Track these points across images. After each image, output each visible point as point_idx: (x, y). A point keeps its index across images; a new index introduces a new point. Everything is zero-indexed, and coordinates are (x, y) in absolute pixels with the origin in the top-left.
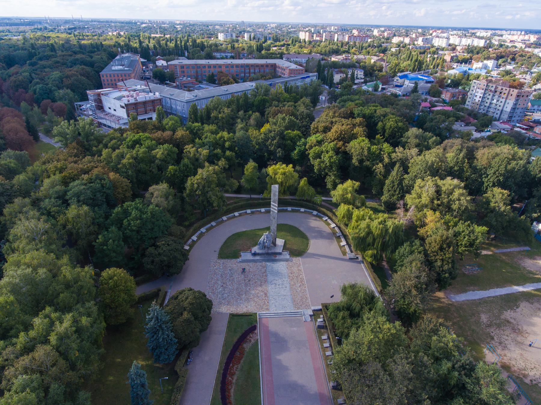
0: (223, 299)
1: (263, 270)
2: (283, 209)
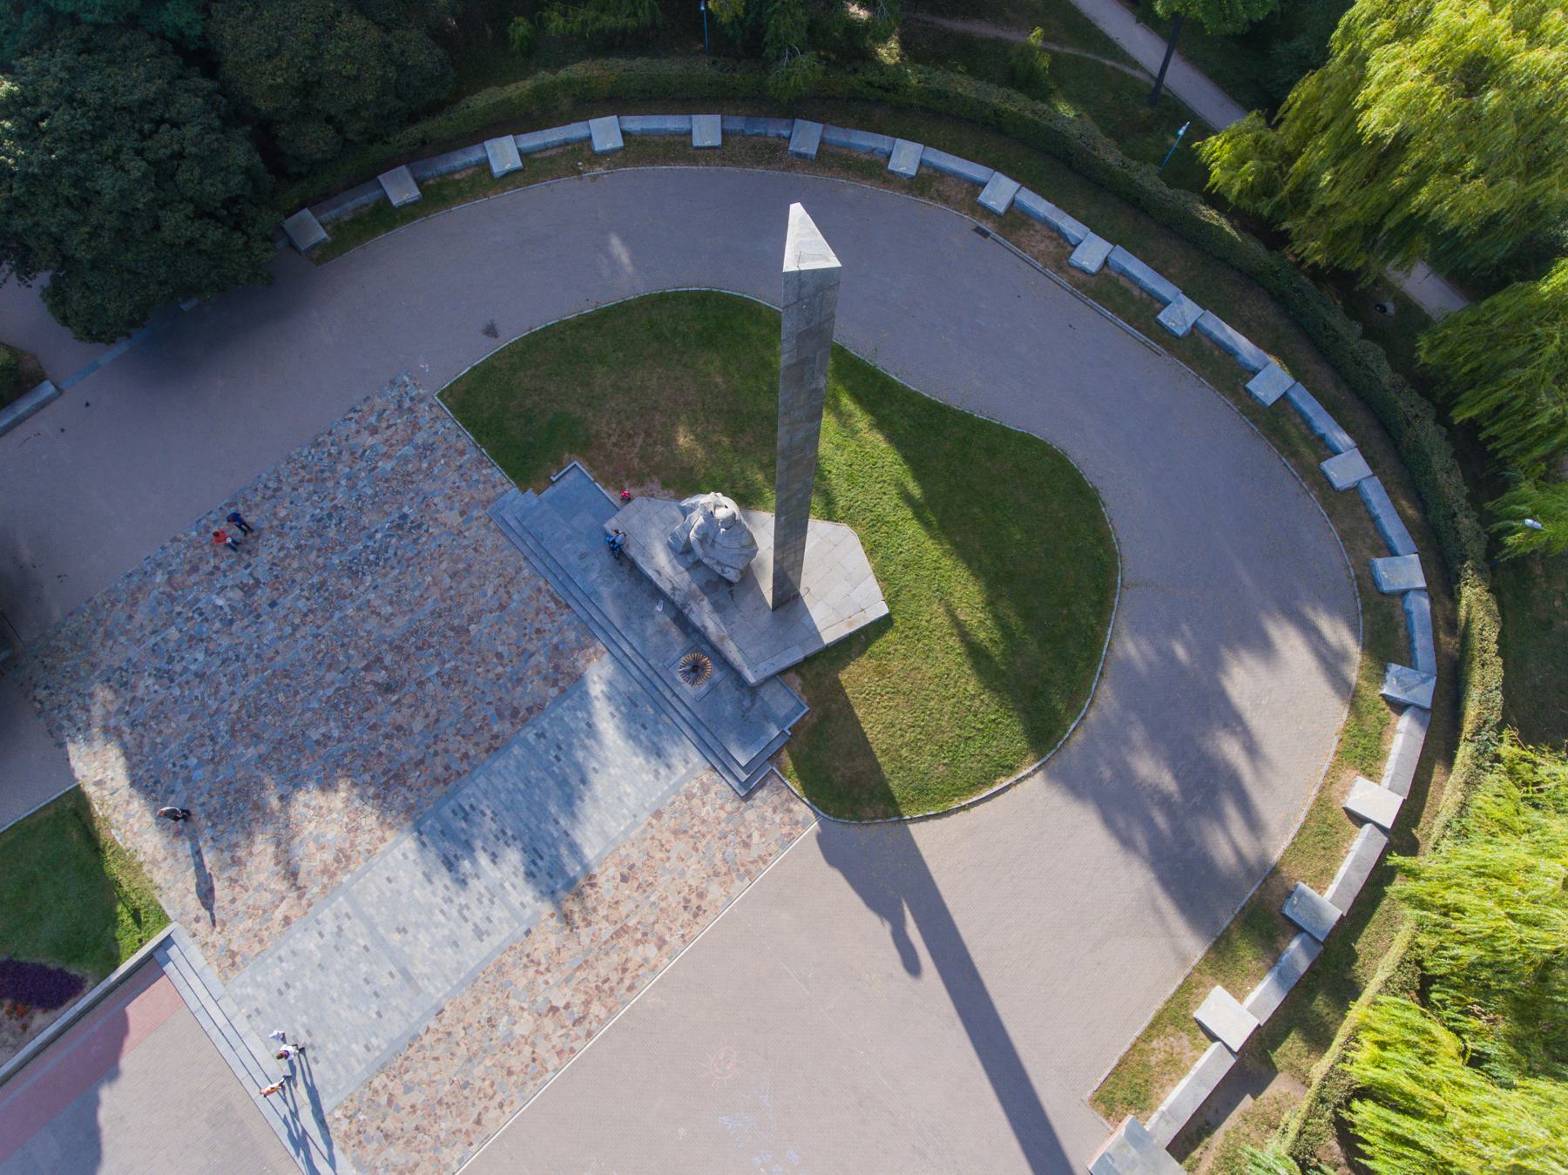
0: (159, 674)
1: (522, 697)
2: (1230, 353)
